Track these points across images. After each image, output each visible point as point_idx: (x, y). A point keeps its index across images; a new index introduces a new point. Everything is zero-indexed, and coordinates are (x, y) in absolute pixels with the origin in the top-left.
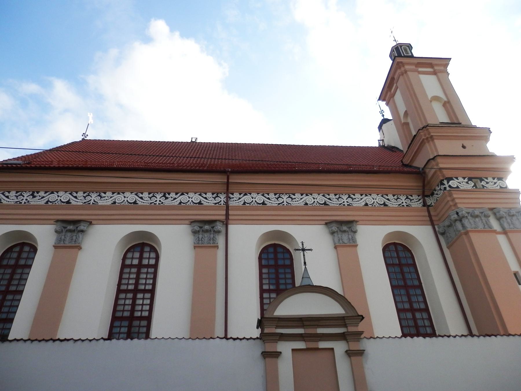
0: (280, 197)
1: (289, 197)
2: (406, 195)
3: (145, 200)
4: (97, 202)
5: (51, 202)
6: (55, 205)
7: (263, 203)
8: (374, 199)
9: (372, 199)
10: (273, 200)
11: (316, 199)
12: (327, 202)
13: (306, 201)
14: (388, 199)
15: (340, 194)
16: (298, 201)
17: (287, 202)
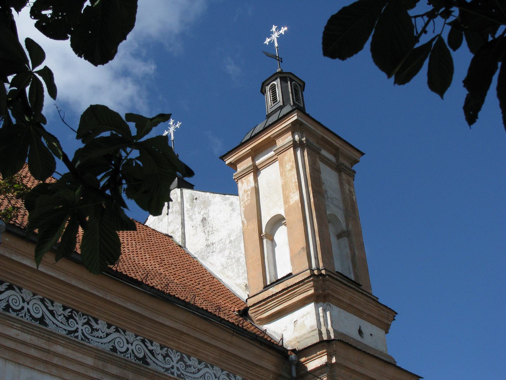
0: (71, 317)
1: (88, 323)
2: (182, 353)
3: (59, 321)
4: (88, 339)
5: (14, 310)
6: (21, 319)
7: (42, 320)
8: (128, 343)
9: (125, 342)
10: (59, 318)
11: (28, 303)
12: (46, 317)
13: (114, 343)
14: (52, 312)
15: (168, 348)
16: (101, 338)
17: (83, 334)
